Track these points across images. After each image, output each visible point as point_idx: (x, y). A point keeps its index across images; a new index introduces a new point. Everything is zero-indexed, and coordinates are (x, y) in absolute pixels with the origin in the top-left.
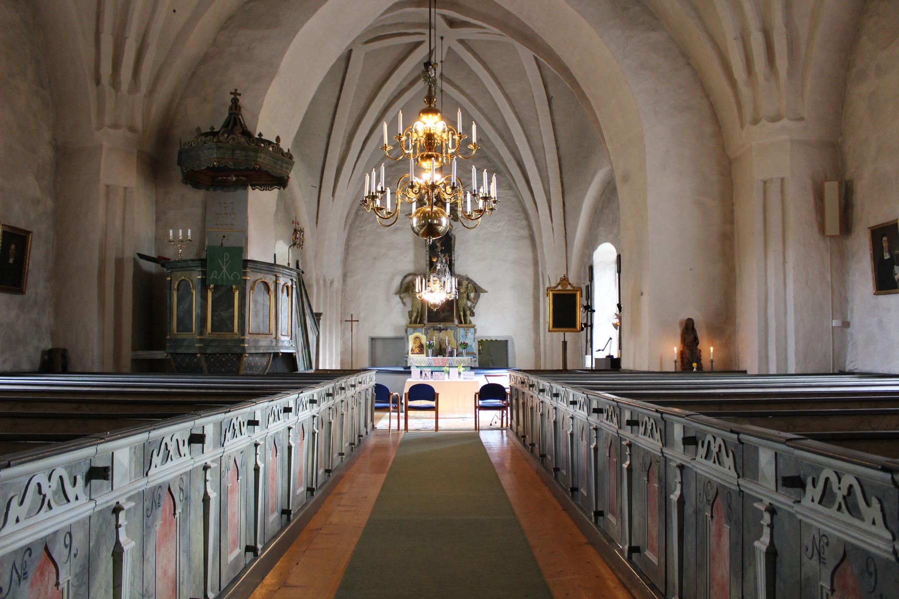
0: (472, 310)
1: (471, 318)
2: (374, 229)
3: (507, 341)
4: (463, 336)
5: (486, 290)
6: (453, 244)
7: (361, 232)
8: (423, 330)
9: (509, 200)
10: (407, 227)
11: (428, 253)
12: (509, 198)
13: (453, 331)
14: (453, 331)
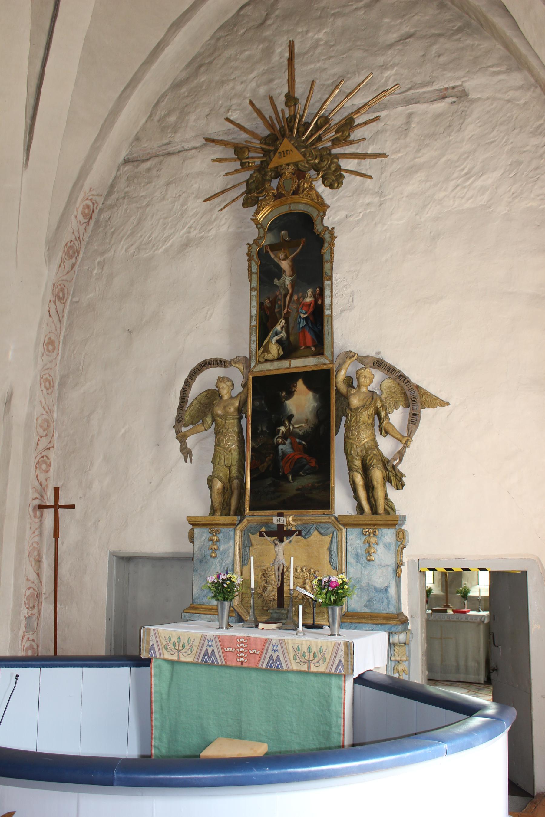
0: (394, 467)
1: (393, 494)
2: (133, 254)
3: (524, 574)
4: (357, 556)
5: (443, 397)
6: (326, 257)
7: (102, 265)
8: (238, 533)
9: (509, 101)
10: (213, 232)
11: (255, 293)
12: (511, 94)
13: (327, 539)
14: (327, 539)
